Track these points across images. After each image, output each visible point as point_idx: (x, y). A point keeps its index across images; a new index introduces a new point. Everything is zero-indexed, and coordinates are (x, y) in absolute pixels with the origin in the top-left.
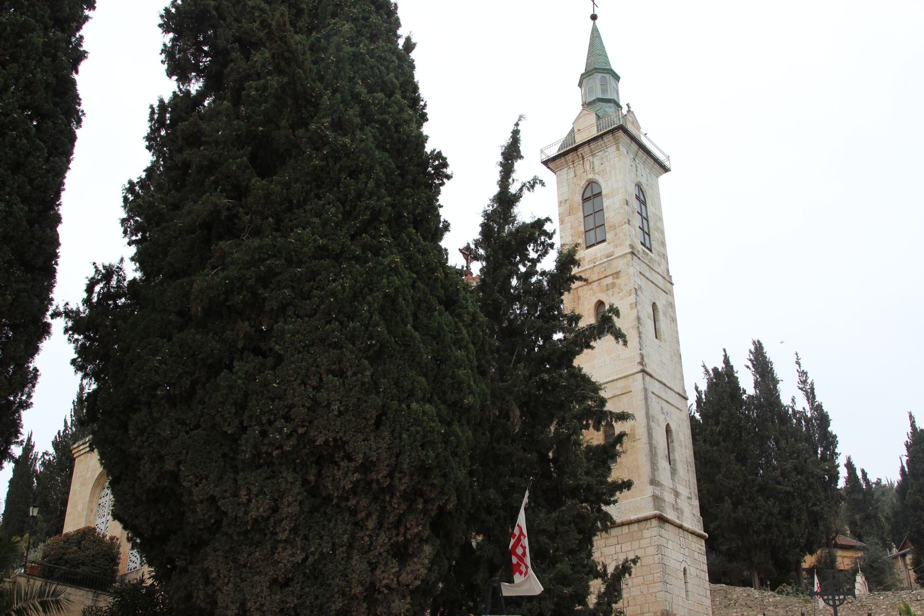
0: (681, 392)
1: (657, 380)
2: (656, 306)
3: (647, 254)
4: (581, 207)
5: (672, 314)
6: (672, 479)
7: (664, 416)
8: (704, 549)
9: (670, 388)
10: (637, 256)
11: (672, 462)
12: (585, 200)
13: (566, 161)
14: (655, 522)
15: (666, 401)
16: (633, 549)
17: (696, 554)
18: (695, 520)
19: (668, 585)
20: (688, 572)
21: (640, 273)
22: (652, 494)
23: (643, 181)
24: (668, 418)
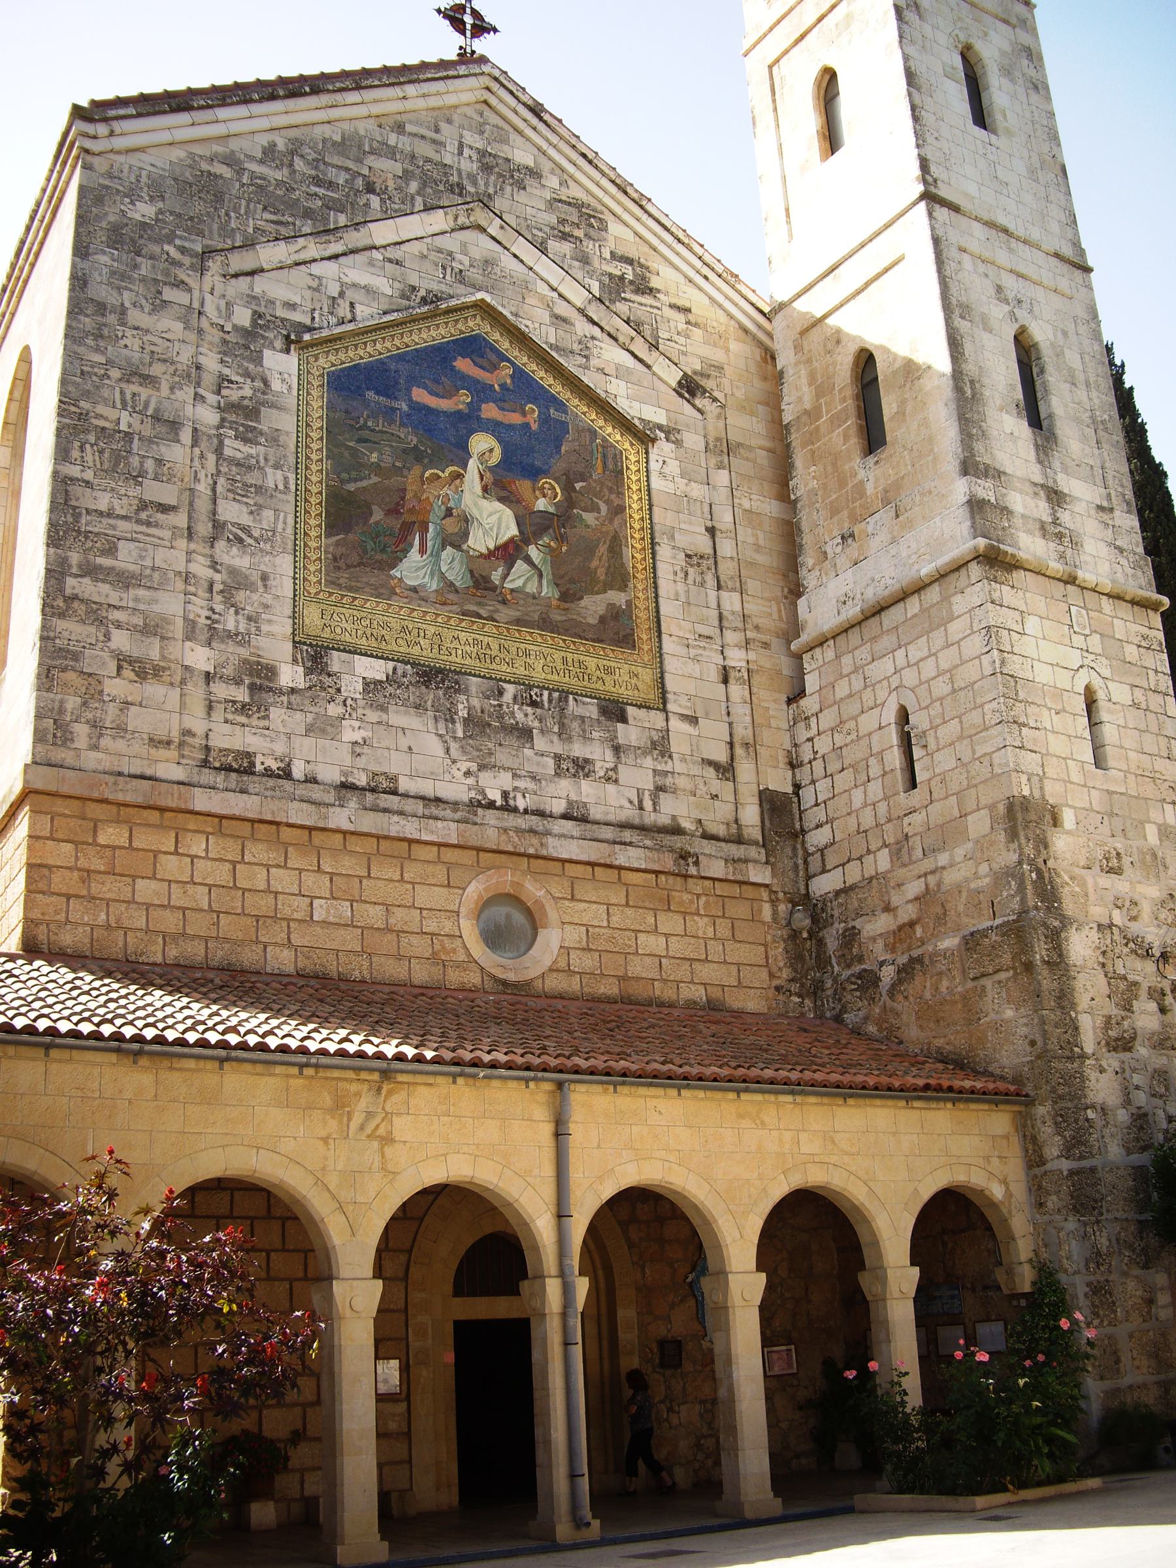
0: (1067, 251)
1: (976, 219)
2: (976, 54)
5: (1032, 72)
6: (1040, 462)
7: (1007, 308)
8: (1161, 636)
9: (1025, 242)
11: (1045, 424)
14: (975, 570)
16: (933, 651)
17: (1131, 652)
18: (1124, 562)
20: (1101, 695)
22: (965, 499)
24: (1022, 315)
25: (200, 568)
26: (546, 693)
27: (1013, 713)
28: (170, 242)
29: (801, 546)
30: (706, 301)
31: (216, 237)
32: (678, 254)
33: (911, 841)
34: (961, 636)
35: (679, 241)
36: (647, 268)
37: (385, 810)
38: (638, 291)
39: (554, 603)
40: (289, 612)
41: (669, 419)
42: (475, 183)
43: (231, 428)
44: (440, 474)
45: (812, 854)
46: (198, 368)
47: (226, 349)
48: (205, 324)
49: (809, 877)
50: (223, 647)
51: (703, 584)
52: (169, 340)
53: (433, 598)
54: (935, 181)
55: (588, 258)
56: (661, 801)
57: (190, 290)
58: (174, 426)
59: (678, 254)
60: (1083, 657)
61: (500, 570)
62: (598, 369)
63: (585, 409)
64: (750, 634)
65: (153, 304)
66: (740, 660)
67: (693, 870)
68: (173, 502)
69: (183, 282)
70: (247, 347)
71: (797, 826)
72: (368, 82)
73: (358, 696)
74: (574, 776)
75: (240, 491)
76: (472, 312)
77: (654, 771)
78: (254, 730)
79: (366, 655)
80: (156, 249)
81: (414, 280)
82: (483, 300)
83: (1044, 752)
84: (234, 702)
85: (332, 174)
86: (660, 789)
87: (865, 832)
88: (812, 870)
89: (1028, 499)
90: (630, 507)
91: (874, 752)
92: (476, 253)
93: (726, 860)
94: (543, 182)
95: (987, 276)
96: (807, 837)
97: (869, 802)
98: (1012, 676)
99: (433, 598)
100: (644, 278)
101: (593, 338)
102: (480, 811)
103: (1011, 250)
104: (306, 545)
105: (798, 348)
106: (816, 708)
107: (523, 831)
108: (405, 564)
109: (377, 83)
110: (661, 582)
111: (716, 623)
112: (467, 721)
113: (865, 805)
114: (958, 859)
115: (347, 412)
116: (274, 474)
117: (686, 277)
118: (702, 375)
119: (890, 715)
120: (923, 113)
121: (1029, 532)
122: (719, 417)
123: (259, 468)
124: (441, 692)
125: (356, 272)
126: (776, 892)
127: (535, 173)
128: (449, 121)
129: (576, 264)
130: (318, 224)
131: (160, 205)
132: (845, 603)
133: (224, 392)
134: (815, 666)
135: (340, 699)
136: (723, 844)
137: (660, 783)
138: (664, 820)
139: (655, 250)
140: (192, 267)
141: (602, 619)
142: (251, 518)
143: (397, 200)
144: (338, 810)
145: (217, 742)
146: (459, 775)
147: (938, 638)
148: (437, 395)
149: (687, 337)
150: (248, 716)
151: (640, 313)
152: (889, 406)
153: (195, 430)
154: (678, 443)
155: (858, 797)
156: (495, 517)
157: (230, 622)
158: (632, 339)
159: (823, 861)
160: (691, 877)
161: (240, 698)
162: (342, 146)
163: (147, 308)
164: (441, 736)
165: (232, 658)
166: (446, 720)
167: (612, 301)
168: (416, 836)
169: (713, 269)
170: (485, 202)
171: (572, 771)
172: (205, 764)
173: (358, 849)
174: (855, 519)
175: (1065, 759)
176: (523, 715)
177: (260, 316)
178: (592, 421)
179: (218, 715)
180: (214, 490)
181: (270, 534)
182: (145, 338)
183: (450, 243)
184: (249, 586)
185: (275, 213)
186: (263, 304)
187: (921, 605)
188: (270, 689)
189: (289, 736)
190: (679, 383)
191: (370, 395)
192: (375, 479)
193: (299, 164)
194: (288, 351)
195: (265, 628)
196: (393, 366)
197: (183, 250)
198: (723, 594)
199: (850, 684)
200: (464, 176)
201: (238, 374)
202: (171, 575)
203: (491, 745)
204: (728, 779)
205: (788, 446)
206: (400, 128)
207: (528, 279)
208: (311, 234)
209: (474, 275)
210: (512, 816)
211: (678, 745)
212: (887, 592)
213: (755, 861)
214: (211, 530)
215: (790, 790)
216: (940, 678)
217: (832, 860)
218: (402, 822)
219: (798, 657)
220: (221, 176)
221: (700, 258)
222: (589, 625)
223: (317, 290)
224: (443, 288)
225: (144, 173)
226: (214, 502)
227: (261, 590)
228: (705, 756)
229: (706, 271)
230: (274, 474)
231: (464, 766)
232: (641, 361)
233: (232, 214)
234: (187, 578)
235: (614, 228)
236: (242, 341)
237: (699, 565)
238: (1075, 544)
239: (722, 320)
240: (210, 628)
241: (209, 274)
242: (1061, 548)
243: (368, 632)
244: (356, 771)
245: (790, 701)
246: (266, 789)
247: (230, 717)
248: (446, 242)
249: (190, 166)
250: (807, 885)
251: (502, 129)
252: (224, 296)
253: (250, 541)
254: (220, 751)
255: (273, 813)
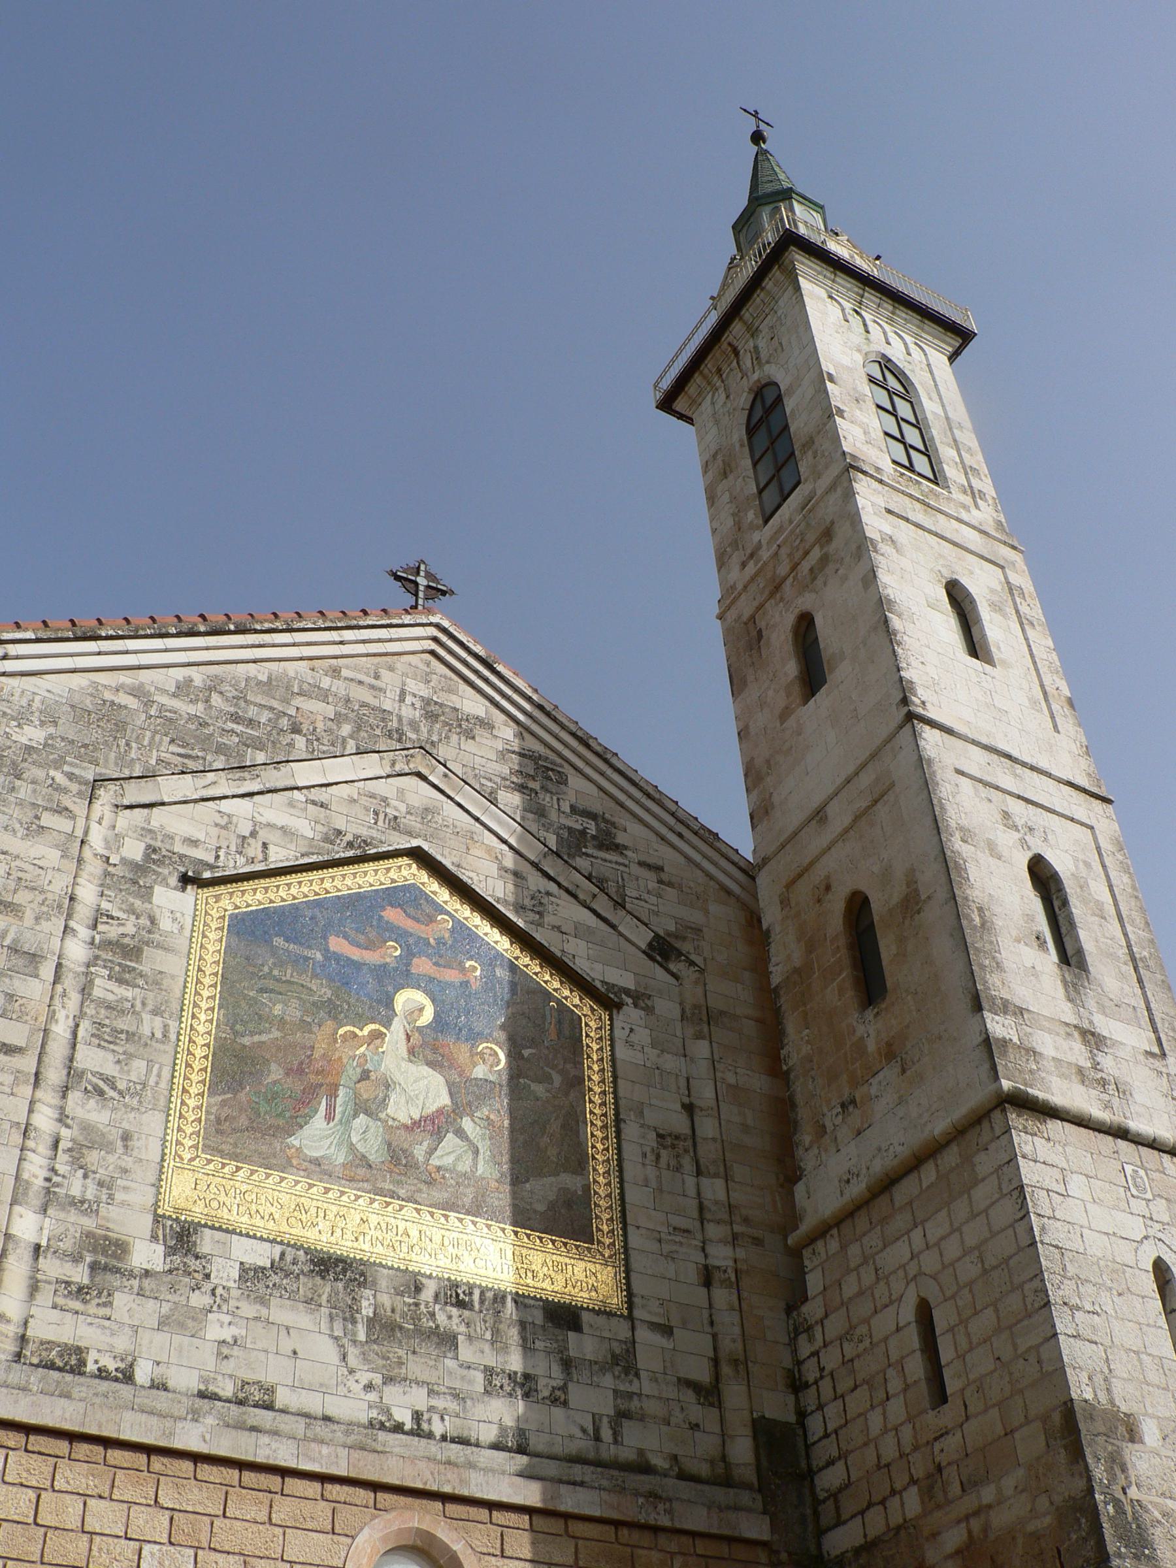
1: (974, 742)
2: (963, 589)
3: (920, 483)
4: (746, 449)
6: (1070, 1000)
7: (1017, 836)
9: (1033, 768)
10: (872, 476)
11: (1073, 961)
12: (751, 431)
13: (705, 377)
15: (1019, 797)
16: (956, 1225)
19: (1079, 1315)
21: (889, 511)
22: (980, 1039)
23: (896, 352)
25: (44, 1120)
26: (477, 1293)
27: (1061, 1293)
28: (56, 769)
29: (796, 1122)
30: (682, 860)
31: (112, 765)
32: (648, 810)
33: (945, 1473)
34: (988, 1202)
35: (649, 796)
36: (613, 824)
37: (253, 1429)
38: (601, 847)
39: (494, 1184)
40: (152, 1179)
41: (637, 983)
42: (416, 730)
43: (105, 967)
44: (357, 1031)
45: (824, 1501)
46: (72, 899)
47: (107, 881)
48: (87, 853)
49: (821, 1532)
50: (62, 1215)
51: (678, 1168)
52: (41, 868)
53: (339, 1171)
54: (923, 703)
55: (544, 810)
56: (625, 1431)
57: (74, 818)
58: (34, 958)
59: (648, 810)
60: (1146, 1226)
61: (425, 1144)
62: (554, 927)
63: (538, 969)
64: (737, 1228)
65: (28, 829)
66: (725, 1258)
67: (665, 1521)
68: (21, 1043)
69: (67, 809)
70: (135, 882)
71: (803, 1464)
72: (301, 625)
73: (231, 1284)
74: (510, 1395)
75: (105, 1037)
76: (405, 861)
77: (615, 1391)
78: (89, 1320)
79: (248, 1235)
80: (40, 773)
81: (340, 824)
82: (419, 847)
83: (1107, 1342)
84: (68, 1283)
85: (252, 712)
86: (622, 1415)
87: (888, 1465)
88: (825, 1521)
89: (1060, 1041)
90: (590, 1079)
91: (892, 1360)
92: (416, 801)
93: (709, 1508)
94: (495, 732)
95: (990, 801)
96: (817, 1481)
97: (889, 1426)
98: (1057, 1247)
99: (339, 1171)
100: (608, 833)
101: (548, 894)
102: (382, 1436)
103: (1016, 775)
104: (183, 1103)
105: (785, 902)
106: (820, 1313)
107: (440, 1462)
108: (307, 1131)
109: (310, 626)
110: (627, 1165)
111: (695, 1214)
112: (371, 1322)
113: (885, 1431)
114: (1009, 1492)
115: (247, 959)
116: (152, 1021)
117: (657, 834)
118: (677, 937)
119: (908, 1313)
120: (905, 638)
121: (1062, 1076)
122: (696, 982)
123: (138, 1014)
124: (340, 1285)
125: (272, 810)
126: (777, 1552)
127: (486, 724)
128: (391, 669)
129: (531, 816)
130: (232, 760)
131: (52, 730)
132: (848, 1181)
133: (100, 928)
134: (816, 1262)
135: (207, 1287)
136: (706, 1488)
137: (622, 1407)
138: (626, 1454)
139: (622, 805)
140: (80, 794)
141: (552, 1206)
142: (118, 1067)
143: (326, 742)
144: (188, 1425)
145: (38, 1331)
146: (357, 1388)
147: (961, 1209)
148: (358, 946)
149: (659, 896)
150: (85, 1302)
151: (603, 870)
152: (887, 948)
153: (59, 966)
154: (649, 1010)
155: (875, 1421)
156: (422, 1084)
157: (76, 1187)
158: (594, 896)
159: (837, 1509)
160: (664, 1529)
161: (76, 1278)
162: (268, 686)
163: (21, 832)
164: (336, 1338)
165: (72, 1230)
166: (345, 1319)
167: (573, 857)
168: (292, 1463)
169: (688, 827)
170: (426, 750)
171: (508, 1389)
172: (18, 1356)
173: (212, 1479)
174: (855, 1083)
175: (1137, 1353)
176: (448, 1318)
177: (154, 851)
178: (546, 982)
179: (45, 1297)
180: (75, 1034)
181: (139, 1087)
182: (13, 864)
183: (381, 788)
184: (108, 1147)
185: (183, 747)
186: (160, 838)
187: (938, 1172)
188: (118, 1271)
189: (135, 1329)
190: (650, 945)
191: (279, 941)
192: (276, 1034)
193: (216, 700)
194: (184, 889)
195: (119, 1196)
196: (309, 913)
197: (71, 776)
198: (705, 1182)
199: (859, 1279)
200: (405, 723)
201: (121, 909)
202: (7, 1126)
203: (401, 1352)
204: (712, 1405)
205: (777, 1013)
206: (335, 672)
207: (474, 829)
208: (223, 770)
209: (412, 822)
210: (424, 1441)
211: (646, 1360)
212: (896, 1162)
213: (749, 1510)
214: (64, 1078)
215: (792, 1419)
216: (967, 1259)
217: (849, 1506)
218: (274, 1445)
219: (796, 1254)
220: (126, 707)
221: (673, 814)
222: (535, 1211)
223: (225, 827)
224: (374, 833)
225: (37, 698)
226: (74, 1046)
227: (120, 1150)
228: (681, 1375)
229: (680, 828)
230: (152, 1021)
231: (365, 1377)
232: (605, 920)
233: (134, 745)
234: (26, 1131)
235: (575, 781)
236: (129, 875)
237: (673, 1147)
238: (1122, 1090)
239: (700, 881)
240: (48, 1191)
241: (99, 802)
242: (1106, 1097)
243: (254, 1207)
244: (220, 1378)
245: (790, 1309)
246: (96, 1394)
247: (60, 1301)
248: (381, 788)
249: (91, 695)
250: (819, 1546)
251: (451, 679)
252: (114, 827)
253: (112, 1093)
254: (42, 1343)
255: (100, 1426)
